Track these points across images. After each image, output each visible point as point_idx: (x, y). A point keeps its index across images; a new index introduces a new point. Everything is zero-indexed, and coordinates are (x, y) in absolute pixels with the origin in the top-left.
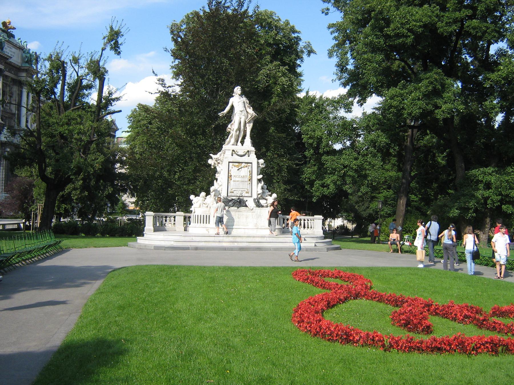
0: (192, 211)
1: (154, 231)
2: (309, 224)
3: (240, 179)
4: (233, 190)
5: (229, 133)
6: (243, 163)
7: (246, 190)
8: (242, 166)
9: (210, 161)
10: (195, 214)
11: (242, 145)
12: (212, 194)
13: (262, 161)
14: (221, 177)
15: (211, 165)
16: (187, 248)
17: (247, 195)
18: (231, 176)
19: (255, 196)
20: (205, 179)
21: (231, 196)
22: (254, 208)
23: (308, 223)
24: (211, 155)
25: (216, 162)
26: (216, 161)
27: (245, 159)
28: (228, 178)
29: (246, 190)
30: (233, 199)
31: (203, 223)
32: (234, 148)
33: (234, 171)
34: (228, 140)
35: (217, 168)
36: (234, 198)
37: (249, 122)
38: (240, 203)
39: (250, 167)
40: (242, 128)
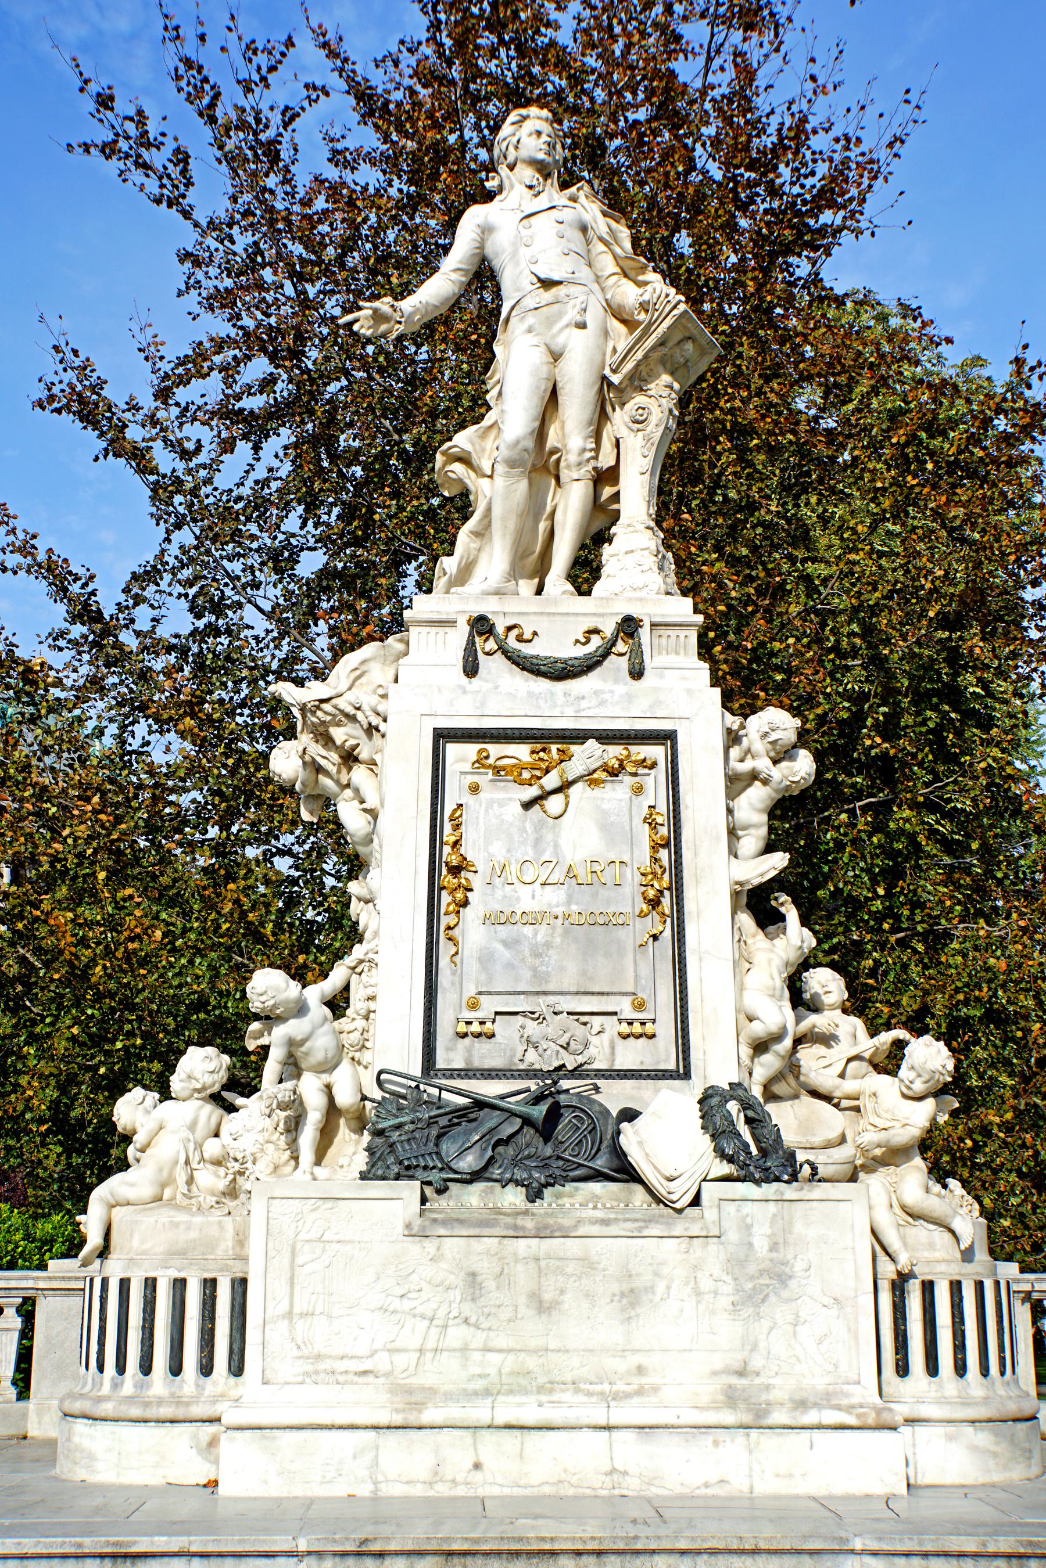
3: (553, 899)
4: (489, 1006)
5: (462, 505)
6: (579, 736)
7: (625, 1007)
10: (115, 1268)
13: (776, 722)
17: (631, 1055)
18: (455, 871)
22: (710, 1191)
27: (603, 699)
29: (625, 1007)
30: (480, 1104)
31: (176, 1368)
33: (493, 820)
36: (490, 1089)
39: (656, 782)
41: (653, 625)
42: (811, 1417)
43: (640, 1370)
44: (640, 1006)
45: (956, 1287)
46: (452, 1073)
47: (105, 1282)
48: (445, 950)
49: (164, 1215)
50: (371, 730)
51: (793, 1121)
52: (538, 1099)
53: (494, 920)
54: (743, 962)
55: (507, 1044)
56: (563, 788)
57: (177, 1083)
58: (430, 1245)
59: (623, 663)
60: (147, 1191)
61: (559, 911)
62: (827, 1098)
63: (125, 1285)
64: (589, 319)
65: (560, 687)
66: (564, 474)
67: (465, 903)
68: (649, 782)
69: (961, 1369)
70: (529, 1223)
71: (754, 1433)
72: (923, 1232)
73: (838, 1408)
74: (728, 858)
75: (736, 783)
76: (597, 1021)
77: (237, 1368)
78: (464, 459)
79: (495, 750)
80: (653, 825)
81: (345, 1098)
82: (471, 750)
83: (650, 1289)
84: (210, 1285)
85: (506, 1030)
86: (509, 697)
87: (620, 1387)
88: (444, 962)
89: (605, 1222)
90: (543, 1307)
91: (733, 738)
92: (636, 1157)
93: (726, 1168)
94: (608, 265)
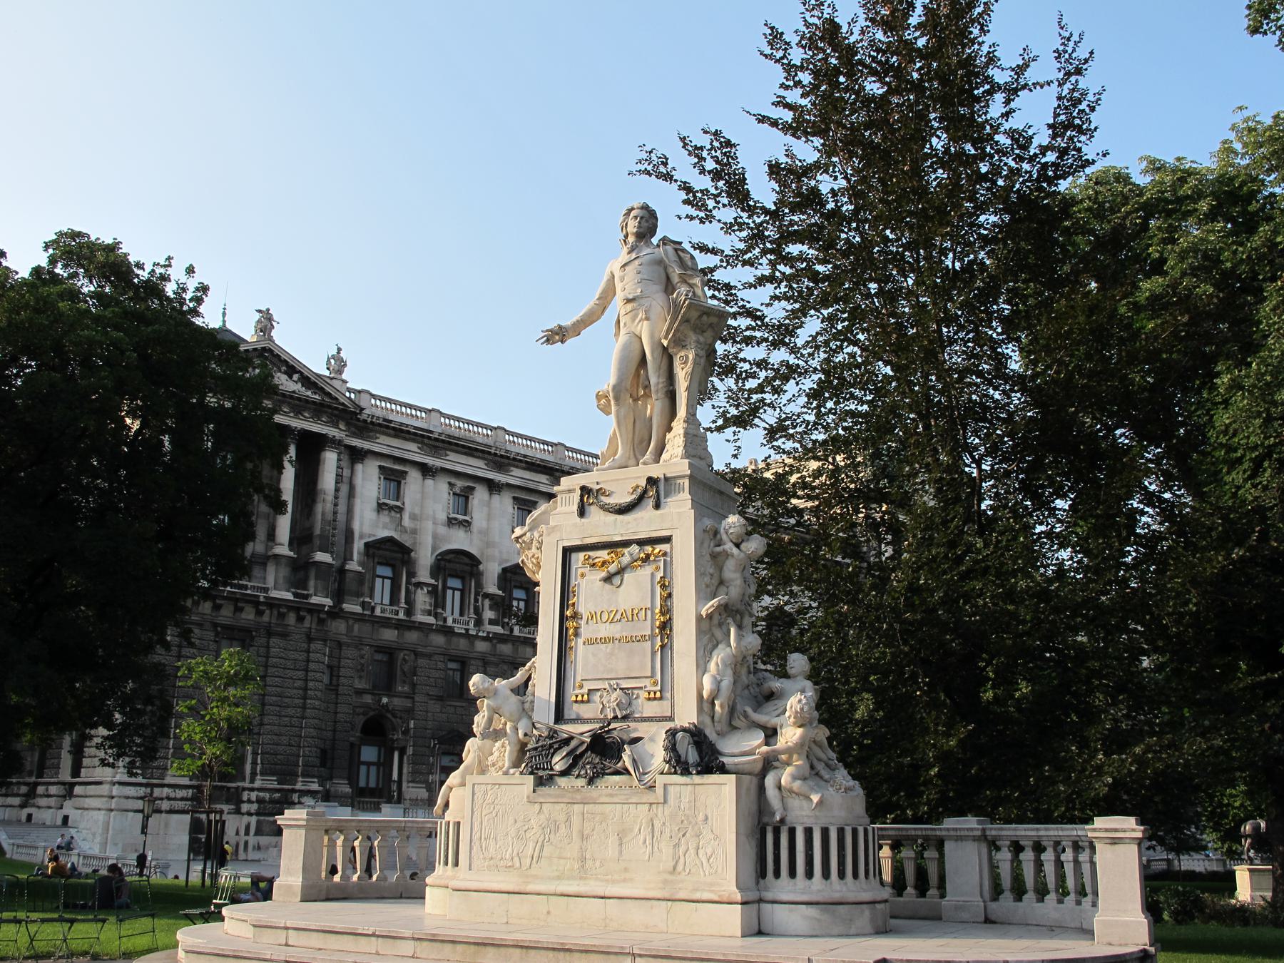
1: (305, 899)
2: (1069, 869)
6: (626, 544)
8: (626, 560)
10: (449, 816)
17: (651, 709)
23: (1076, 862)
41: (666, 479)
42: (697, 896)
43: (626, 870)
45: (809, 832)
56: (621, 571)
58: (537, 806)
59: (650, 503)
61: (617, 636)
64: (652, 316)
65: (621, 517)
67: (576, 634)
69: (809, 874)
70: (578, 797)
71: (670, 903)
73: (712, 891)
76: (636, 692)
79: (590, 553)
80: (663, 587)
82: (581, 555)
83: (632, 830)
87: (616, 877)
89: (611, 795)
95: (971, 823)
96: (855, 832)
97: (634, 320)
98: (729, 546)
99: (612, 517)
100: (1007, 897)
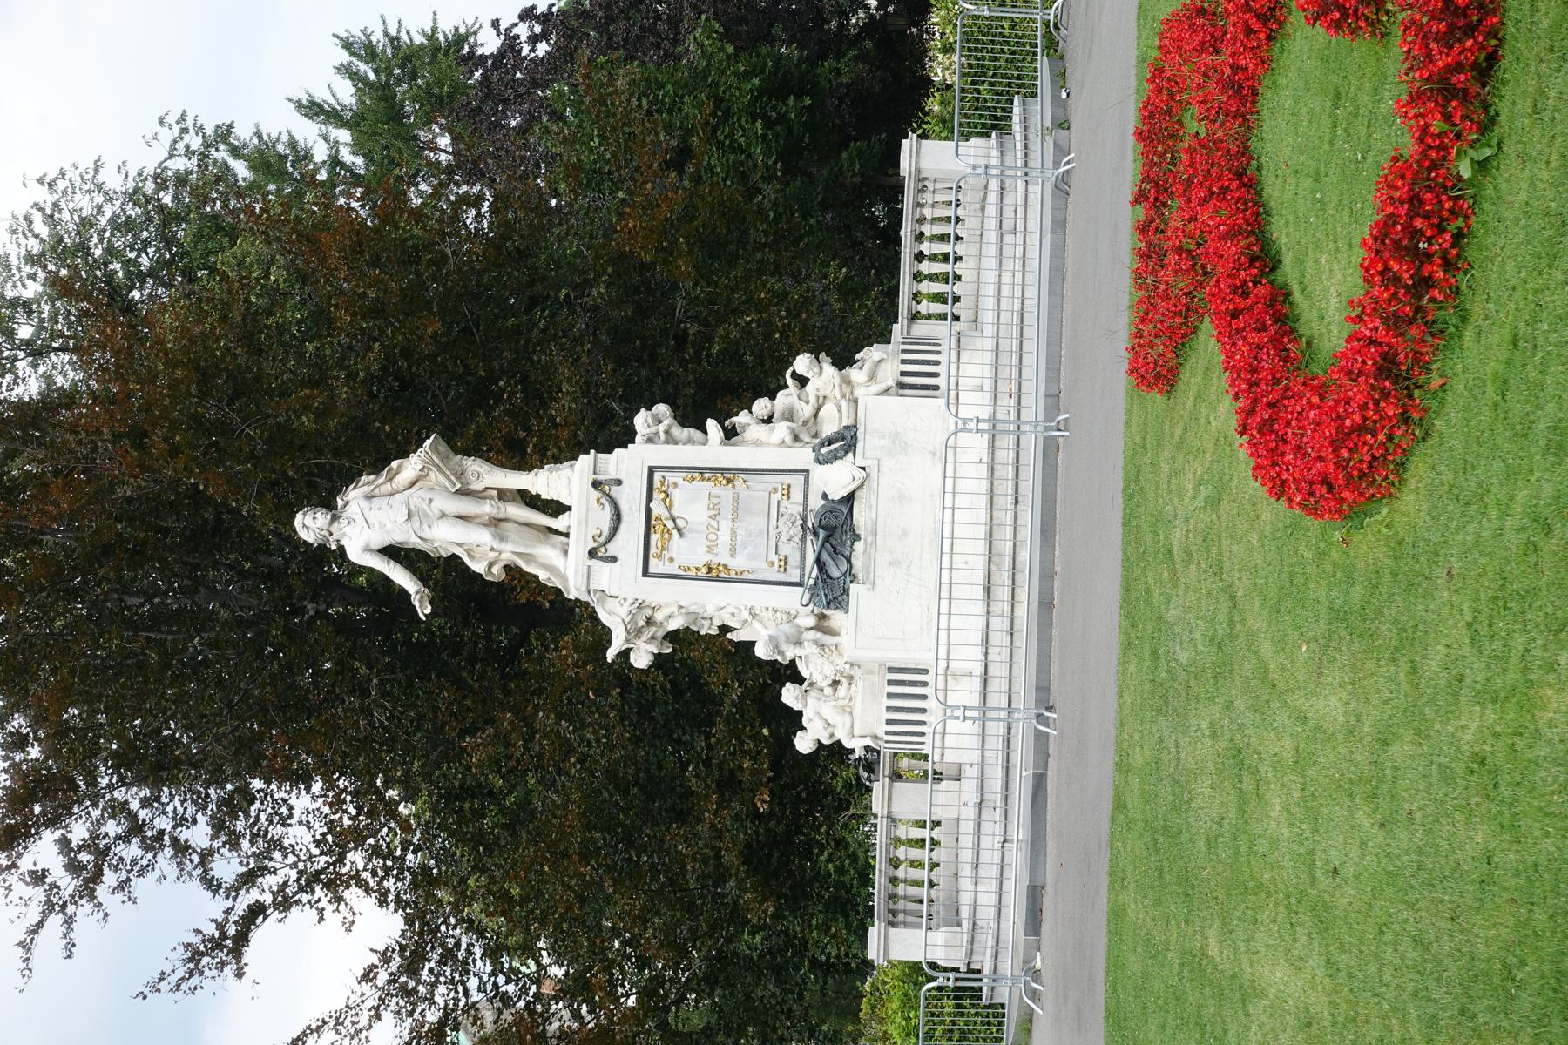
0: (867, 749)
3: (725, 526)
4: (773, 557)
5: (508, 568)
6: (649, 511)
7: (776, 497)
8: (664, 514)
9: (641, 659)
10: (881, 734)
11: (569, 508)
12: (791, 652)
13: (641, 420)
14: (716, 607)
15: (658, 656)
16: (1039, 782)
17: (797, 496)
19: (802, 456)
20: (723, 688)
21: (802, 567)
22: (860, 462)
24: (611, 654)
25: (645, 636)
26: (639, 632)
27: (631, 498)
28: (718, 579)
29: (776, 497)
32: (579, 545)
34: (543, 576)
35: (673, 625)
36: (811, 557)
37: (460, 475)
38: (834, 527)
39: (672, 477)
40: (487, 508)
43: (931, 496)
44: (776, 490)
46: (802, 574)
47: (888, 733)
48: (746, 576)
49: (858, 707)
50: (640, 606)
51: (829, 427)
52: (816, 534)
53: (733, 552)
54: (758, 443)
55: (790, 550)
57: (796, 707)
59: (614, 488)
60: (847, 718)
62: (819, 409)
63: (889, 722)
66: (501, 516)
67: (725, 567)
68: (672, 480)
70: (870, 539)
72: (880, 374)
74: (710, 447)
75: (670, 439)
76: (782, 510)
77: (926, 671)
78: (491, 565)
79: (653, 551)
81: (811, 622)
82: (652, 561)
84: (890, 683)
85: (785, 549)
86: (629, 542)
88: (751, 577)
90: (905, 535)
91: (650, 440)
92: (844, 493)
93: (850, 455)
94: (387, 488)
95: (896, 328)
96: (904, 351)
97: (427, 516)
98: (662, 428)
99: (623, 526)
100: (958, 309)
